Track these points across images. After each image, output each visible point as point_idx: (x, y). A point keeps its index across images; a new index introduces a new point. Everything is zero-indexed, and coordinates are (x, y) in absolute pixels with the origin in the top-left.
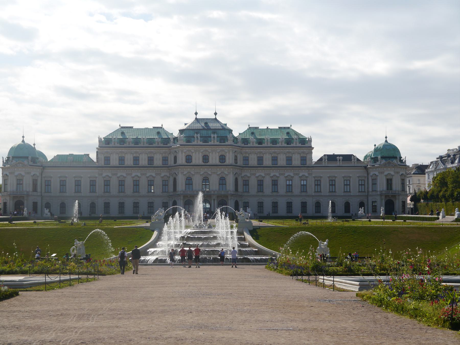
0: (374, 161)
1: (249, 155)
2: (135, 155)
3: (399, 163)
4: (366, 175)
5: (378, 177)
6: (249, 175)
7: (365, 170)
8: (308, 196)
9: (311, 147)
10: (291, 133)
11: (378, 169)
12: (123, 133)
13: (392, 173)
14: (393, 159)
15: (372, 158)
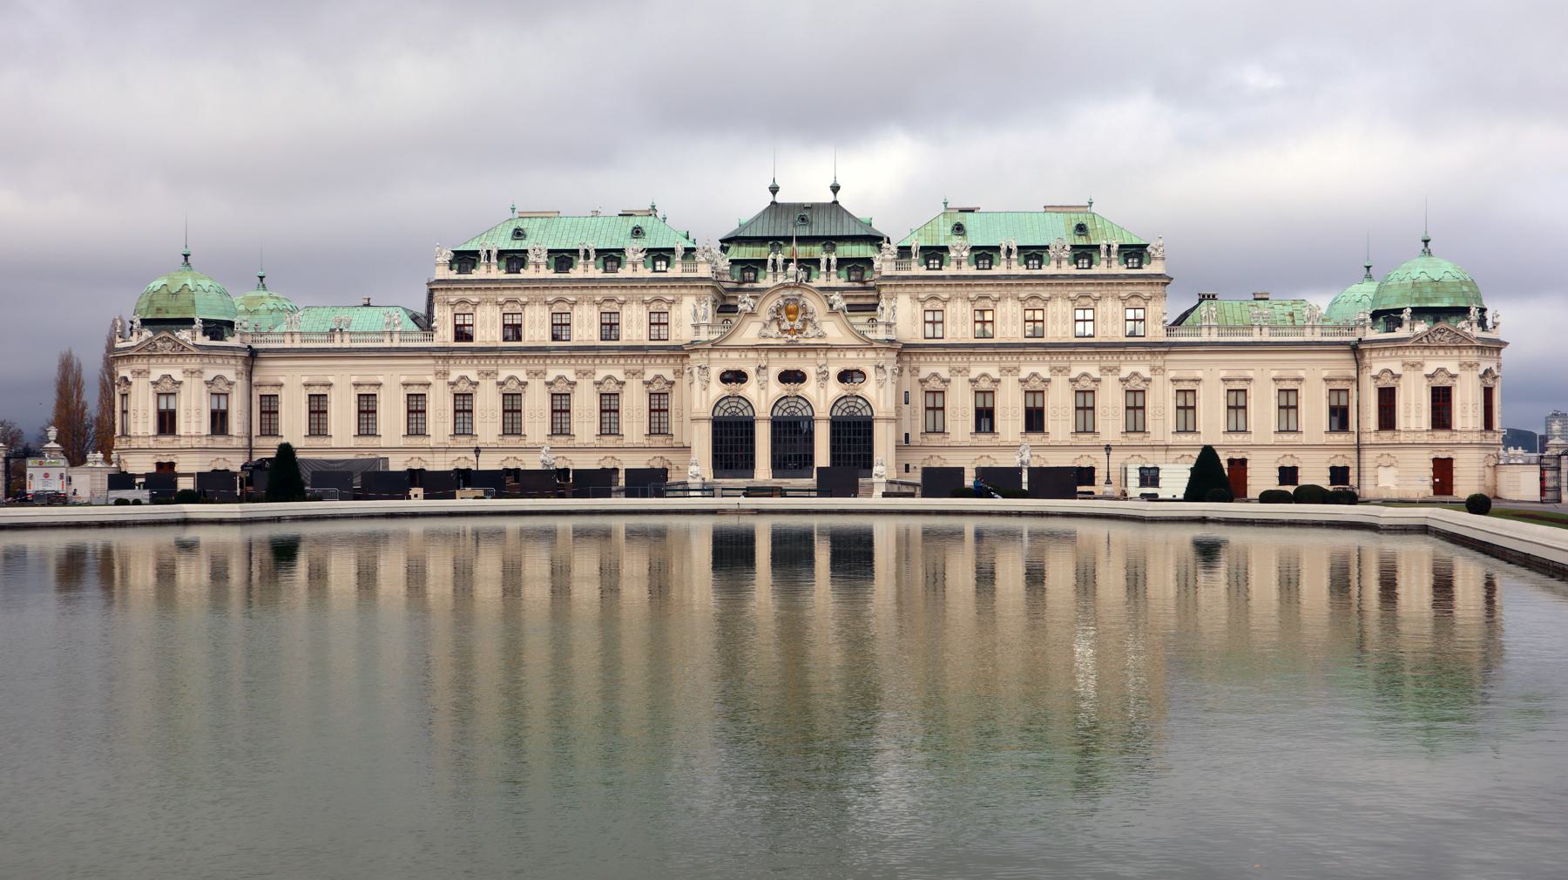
0: (1387, 321)
1: (945, 301)
2: (555, 309)
3: (1477, 332)
4: (1353, 374)
5: (1401, 382)
6: (944, 374)
7: (1349, 356)
8: (1153, 447)
9: (1159, 276)
10: (1089, 227)
11: (1400, 353)
12: (519, 234)
13: (1452, 367)
14: (1453, 320)
15: (1375, 315)
